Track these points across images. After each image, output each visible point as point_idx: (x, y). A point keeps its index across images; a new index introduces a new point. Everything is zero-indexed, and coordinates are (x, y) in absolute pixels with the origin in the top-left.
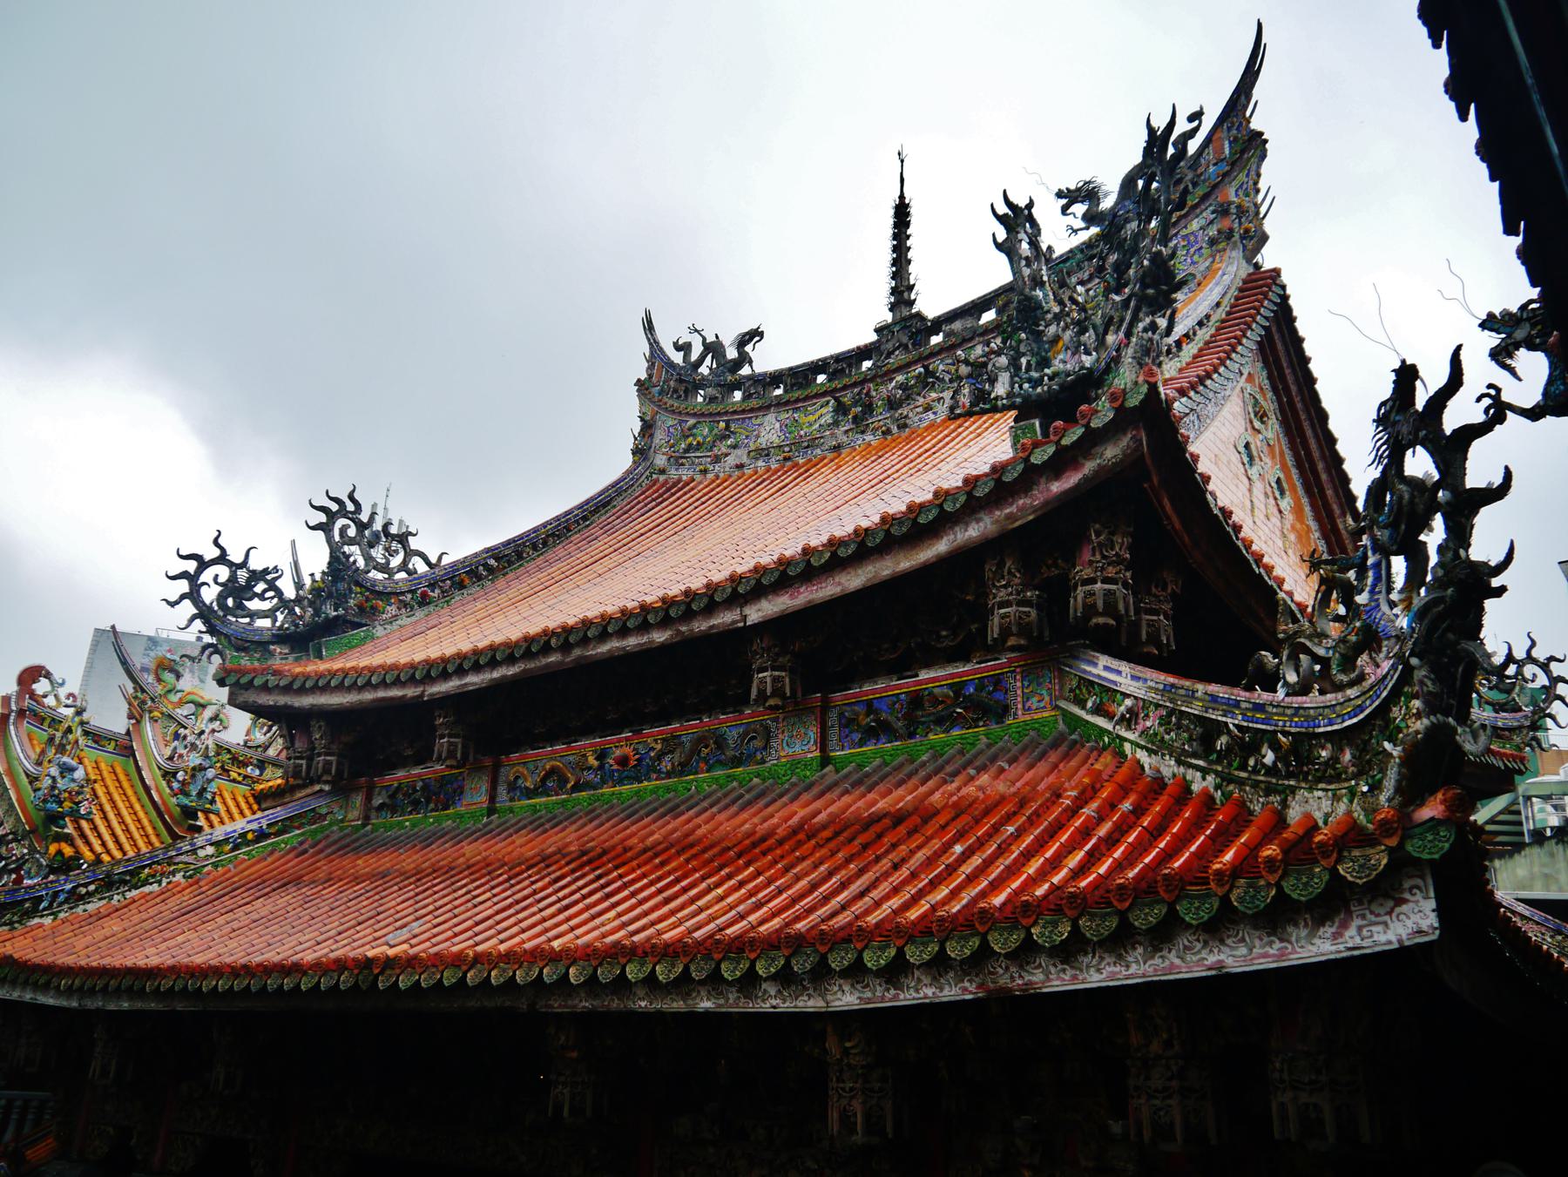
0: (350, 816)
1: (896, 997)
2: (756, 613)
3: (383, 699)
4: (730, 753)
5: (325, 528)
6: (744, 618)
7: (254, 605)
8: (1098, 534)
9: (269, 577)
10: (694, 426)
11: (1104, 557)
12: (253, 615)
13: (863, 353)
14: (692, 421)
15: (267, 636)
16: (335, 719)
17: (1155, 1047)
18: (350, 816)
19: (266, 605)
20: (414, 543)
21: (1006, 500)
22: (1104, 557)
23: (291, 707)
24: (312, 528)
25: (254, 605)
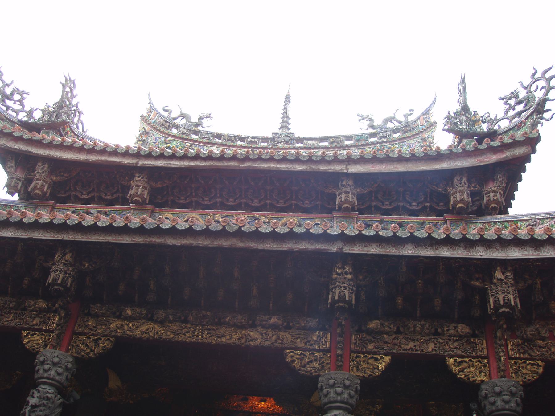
1: (538, 255)
2: (354, 169)
3: (106, 161)
5: (64, 86)
6: (348, 169)
7: (9, 103)
8: (500, 178)
9: (25, 96)
10: (171, 140)
11: (499, 186)
12: (8, 108)
13: (265, 140)
14: (170, 138)
15: (16, 121)
16: (56, 165)
19: (17, 107)
20: (82, 118)
21: (472, 156)
22: (499, 186)
23: (32, 152)
24: (61, 83)
25: (9, 103)
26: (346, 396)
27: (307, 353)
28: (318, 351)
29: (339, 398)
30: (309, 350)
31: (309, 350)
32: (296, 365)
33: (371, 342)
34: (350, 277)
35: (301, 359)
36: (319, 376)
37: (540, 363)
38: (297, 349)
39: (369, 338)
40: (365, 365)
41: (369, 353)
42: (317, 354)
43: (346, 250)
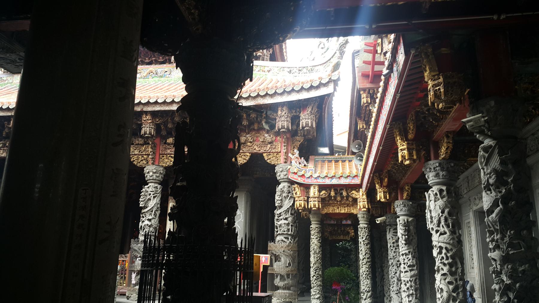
0: (15, 82)
4: (159, 75)
17: (283, 113)
18: (15, 82)
26: (155, 177)
27: (140, 156)
28: (145, 155)
29: (151, 178)
30: (141, 155)
31: (141, 155)
32: (135, 163)
33: (169, 149)
34: (150, 121)
35: (138, 159)
36: (145, 167)
37: (248, 154)
38: (135, 155)
39: (168, 147)
40: (166, 160)
41: (169, 154)
42: (145, 156)
43: (145, 109)
